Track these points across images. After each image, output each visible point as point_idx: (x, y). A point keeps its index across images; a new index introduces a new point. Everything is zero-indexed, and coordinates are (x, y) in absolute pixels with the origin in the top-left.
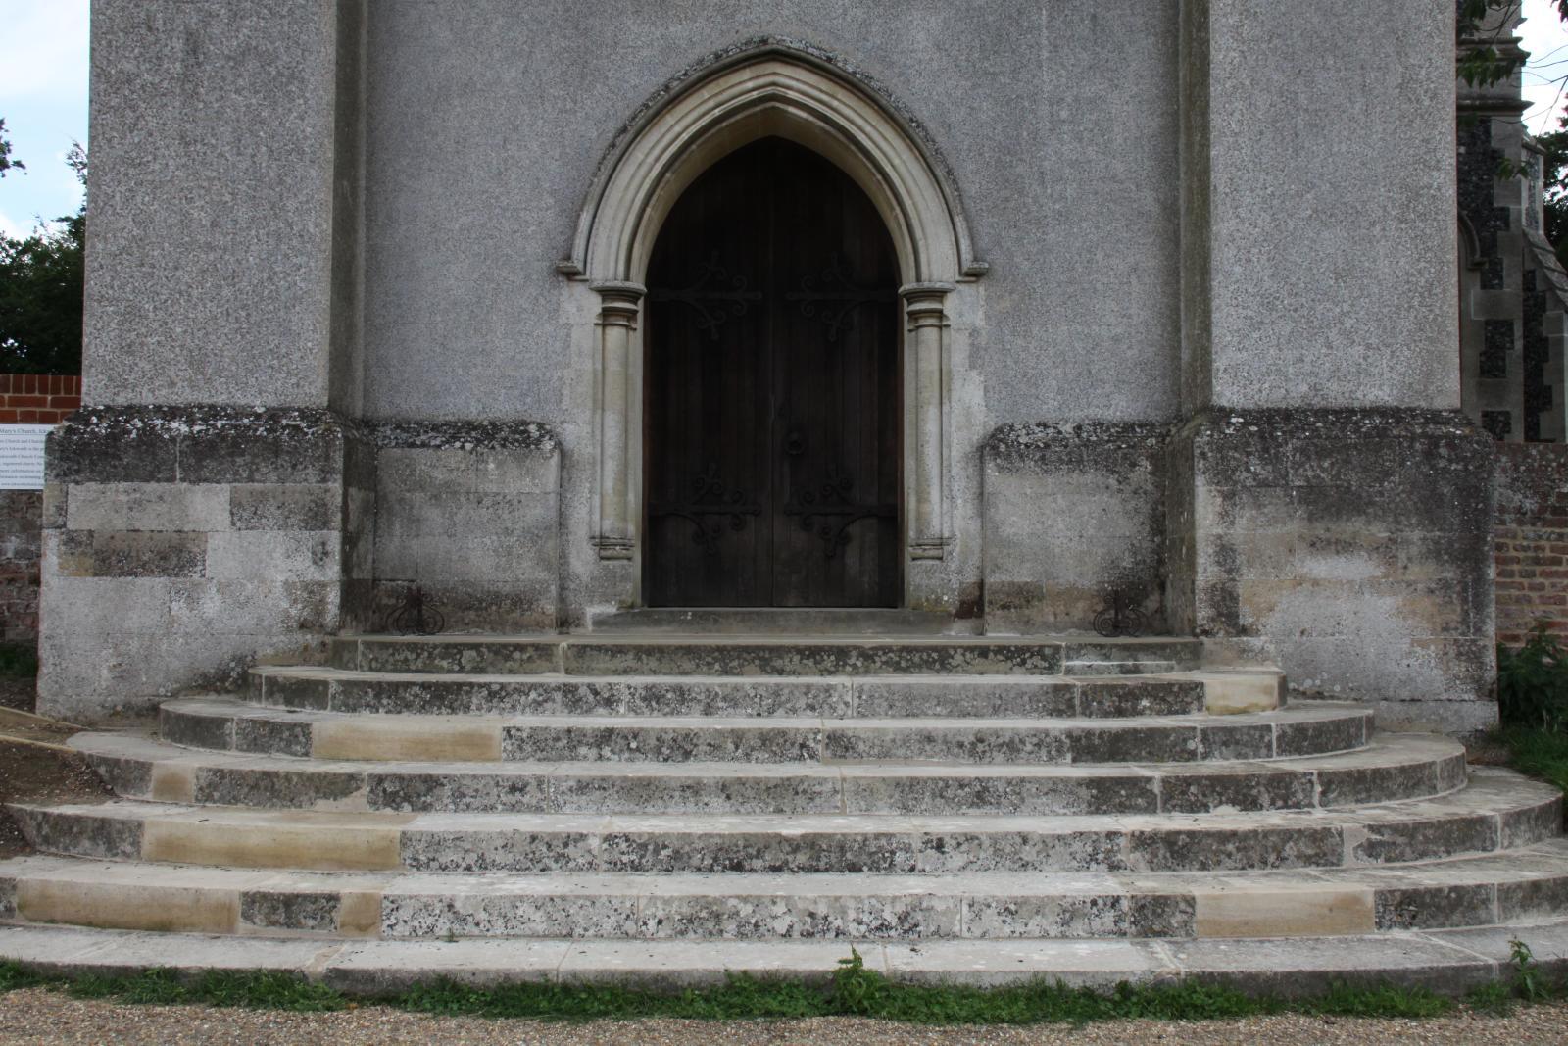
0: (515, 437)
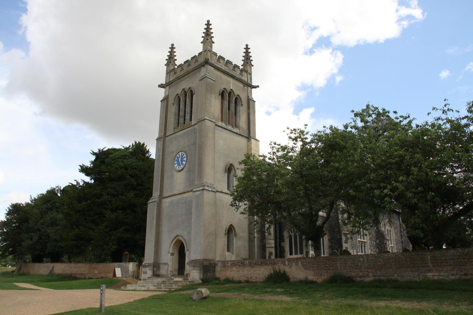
0: (165, 264)
